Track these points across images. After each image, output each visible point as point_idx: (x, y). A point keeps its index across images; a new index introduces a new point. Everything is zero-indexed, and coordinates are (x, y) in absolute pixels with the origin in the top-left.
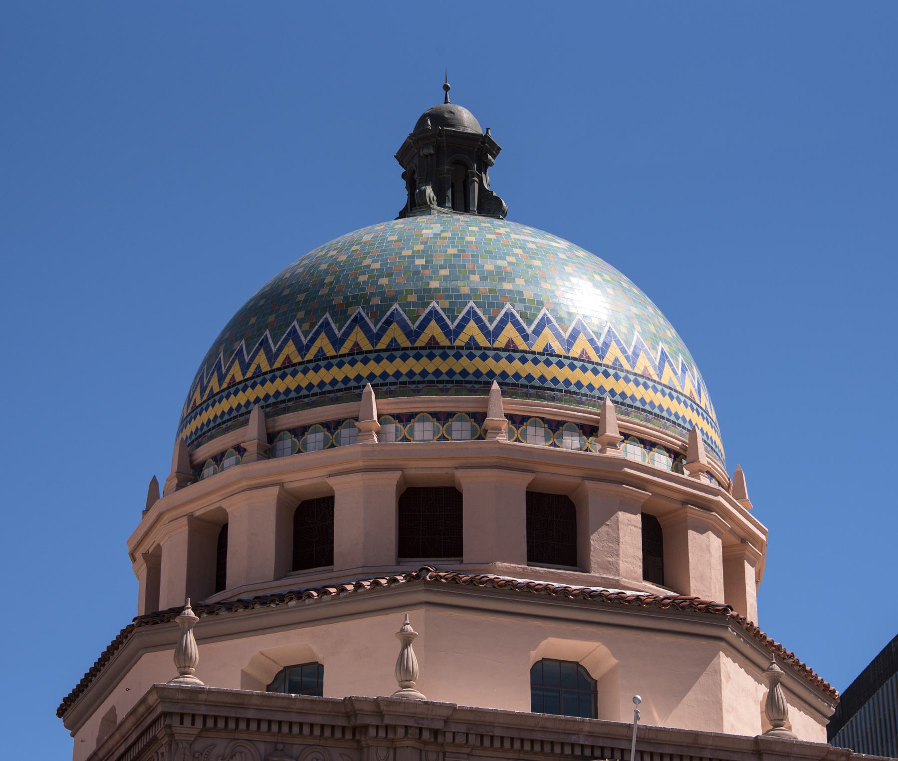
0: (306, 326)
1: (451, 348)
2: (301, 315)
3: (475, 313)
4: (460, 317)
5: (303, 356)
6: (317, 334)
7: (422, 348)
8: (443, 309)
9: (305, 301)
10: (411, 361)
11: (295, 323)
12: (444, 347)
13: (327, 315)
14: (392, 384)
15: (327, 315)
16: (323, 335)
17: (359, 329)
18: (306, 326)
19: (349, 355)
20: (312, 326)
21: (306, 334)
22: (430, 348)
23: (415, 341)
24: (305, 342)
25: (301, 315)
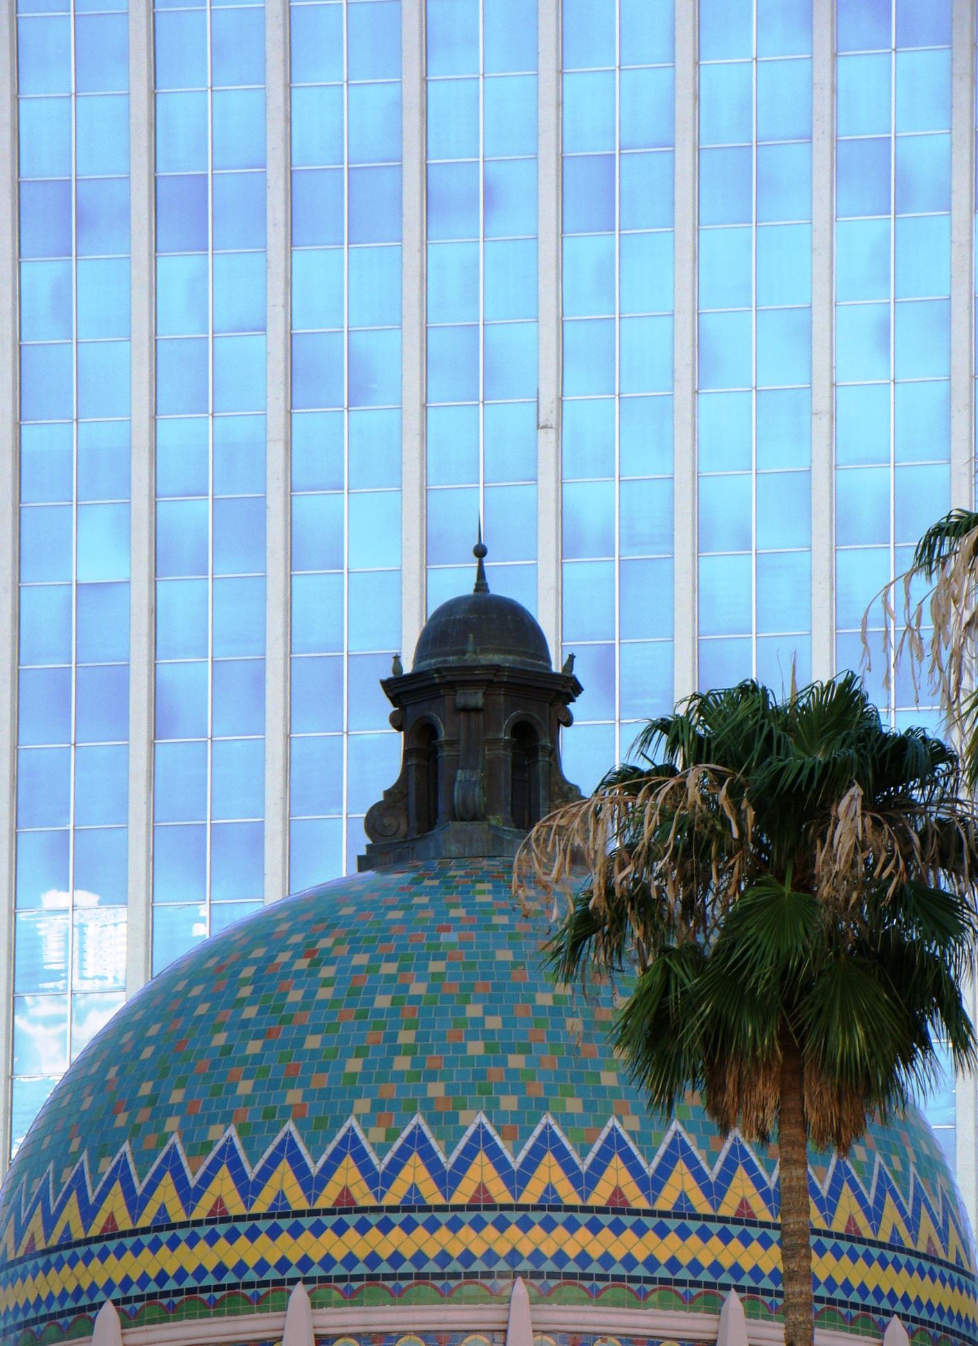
0: (378, 1134)
1: (648, 1213)
2: (363, 1105)
3: (685, 1148)
4: (661, 1151)
5: (379, 1196)
6: (403, 1154)
7: (601, 1210)
8: (632, 1134)
9: (366, 1076)
10: (514, 1232)
11: (352, 1122)
12: (636, 1212)
13: (418, 1119)
14: (552, 1275)
15: (418, 1119)
16: (415, 1159)
17: (486, 1159)
18: (378, 1134)
19: (471, 1208)
20: (392, 1135)
21: (381, 1153)
22: (615, 1211)
23: (520, 1192)
24: (380, 1166)
25: (363, 1105)
